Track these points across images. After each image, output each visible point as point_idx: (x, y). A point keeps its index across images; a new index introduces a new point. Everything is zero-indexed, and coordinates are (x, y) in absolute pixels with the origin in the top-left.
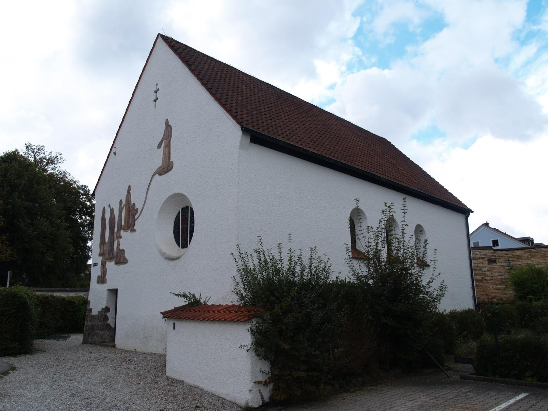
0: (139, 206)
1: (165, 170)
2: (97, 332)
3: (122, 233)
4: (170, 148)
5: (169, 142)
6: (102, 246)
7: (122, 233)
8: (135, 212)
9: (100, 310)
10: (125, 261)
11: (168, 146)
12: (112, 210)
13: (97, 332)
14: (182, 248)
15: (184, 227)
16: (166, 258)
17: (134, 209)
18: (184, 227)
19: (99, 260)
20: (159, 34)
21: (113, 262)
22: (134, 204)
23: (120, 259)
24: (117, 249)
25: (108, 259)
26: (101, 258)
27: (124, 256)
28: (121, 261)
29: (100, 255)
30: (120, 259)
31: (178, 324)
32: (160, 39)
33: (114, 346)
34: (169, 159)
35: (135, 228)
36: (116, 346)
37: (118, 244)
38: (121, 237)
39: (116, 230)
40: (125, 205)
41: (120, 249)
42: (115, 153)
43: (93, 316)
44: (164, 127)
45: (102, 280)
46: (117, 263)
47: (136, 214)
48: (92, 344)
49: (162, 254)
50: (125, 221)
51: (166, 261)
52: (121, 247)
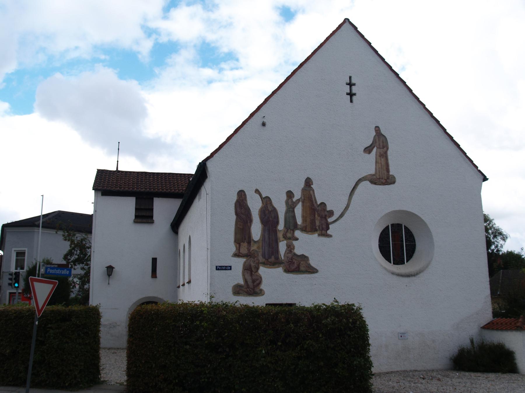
1: (384, 181)
3: (298, 233)
4: (387, 159)
5: (386, 153)
6: (244, 245)
7: (298, 233)
8: (326, 213)
10: (312, 270)
11: (383, 155)
12: (267, 201)
14: (394, 264)
20: (347, 20)
23: (298, 265)
25: (265, 264)
26: (241, 261)
27: (309, 264)
28: (302, 268)
34: (388, 170)
35: (329, 232)
37: (290, 248)
38: (297, 239)
39: (281, 226)
42: (264, 124)
44: (374, 134)
46: (288, 271)
47: (330, 217)
51: (395, 277)
52: (298, 251)
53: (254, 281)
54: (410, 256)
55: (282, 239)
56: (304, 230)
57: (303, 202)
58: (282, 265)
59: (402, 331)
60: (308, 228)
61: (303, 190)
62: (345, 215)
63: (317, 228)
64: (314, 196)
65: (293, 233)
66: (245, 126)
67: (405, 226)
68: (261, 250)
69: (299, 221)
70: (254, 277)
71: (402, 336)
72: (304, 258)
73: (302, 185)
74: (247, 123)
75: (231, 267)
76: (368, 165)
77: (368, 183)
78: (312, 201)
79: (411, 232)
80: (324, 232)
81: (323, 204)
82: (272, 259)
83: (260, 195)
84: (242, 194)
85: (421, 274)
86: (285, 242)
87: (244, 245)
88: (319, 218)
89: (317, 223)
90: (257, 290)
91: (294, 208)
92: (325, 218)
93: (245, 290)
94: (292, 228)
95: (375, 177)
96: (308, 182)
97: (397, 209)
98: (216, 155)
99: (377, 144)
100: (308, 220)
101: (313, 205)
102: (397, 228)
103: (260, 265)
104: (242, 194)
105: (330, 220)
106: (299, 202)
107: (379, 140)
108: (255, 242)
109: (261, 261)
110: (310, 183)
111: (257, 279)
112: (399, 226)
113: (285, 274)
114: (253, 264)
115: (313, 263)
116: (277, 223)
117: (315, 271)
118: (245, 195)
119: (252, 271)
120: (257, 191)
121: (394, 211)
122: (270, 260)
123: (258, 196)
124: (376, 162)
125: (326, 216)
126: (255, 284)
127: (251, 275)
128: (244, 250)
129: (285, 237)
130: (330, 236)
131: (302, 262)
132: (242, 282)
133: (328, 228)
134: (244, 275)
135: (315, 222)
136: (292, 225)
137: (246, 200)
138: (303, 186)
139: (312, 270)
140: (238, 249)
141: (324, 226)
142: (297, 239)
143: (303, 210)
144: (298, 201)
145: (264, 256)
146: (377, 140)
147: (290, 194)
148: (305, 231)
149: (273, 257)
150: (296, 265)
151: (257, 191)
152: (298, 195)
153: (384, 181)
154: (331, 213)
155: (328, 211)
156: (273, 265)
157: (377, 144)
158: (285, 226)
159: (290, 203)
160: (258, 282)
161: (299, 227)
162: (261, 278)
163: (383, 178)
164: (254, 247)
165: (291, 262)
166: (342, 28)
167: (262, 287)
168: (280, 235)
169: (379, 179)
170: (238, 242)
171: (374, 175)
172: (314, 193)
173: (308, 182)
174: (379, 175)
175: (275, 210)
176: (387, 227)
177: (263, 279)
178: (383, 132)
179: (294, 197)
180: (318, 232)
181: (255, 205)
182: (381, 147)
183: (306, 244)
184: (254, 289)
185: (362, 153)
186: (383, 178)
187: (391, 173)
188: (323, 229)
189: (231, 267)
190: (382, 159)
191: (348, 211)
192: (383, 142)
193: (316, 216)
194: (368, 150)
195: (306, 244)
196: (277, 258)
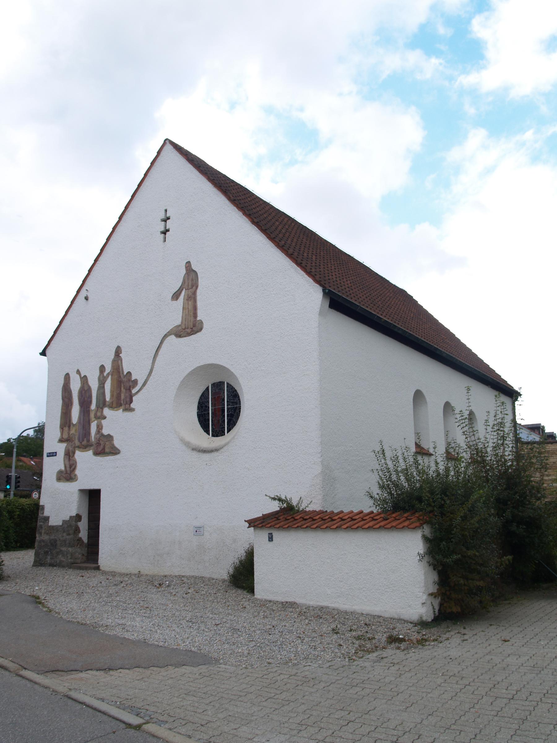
0: (138, 375)
1: (189, 331)
2: (64, 549)
3: (107, 411)
4: (195, 301)
5: (195, 293)
6: (66, 429)
7: (107, 411)
8: (131, 384)
9: (67, 518)
10: (115, 452)
11: (192, 298)
12: (84, 380)
13: (64, 549)
14: (213, 436)
15: (219, 408)
16: (193, 449)
17: (129, 380)
18: (219, 408)
19: (61, 449)
20: (167, 141)
21: (90, 452)
22: (129, 373)
23: (105, 447)
24: (96, 434)
25: (79, 447)
26: (64, 445)
27: (113, 445)
28: (107, 450)
29: (61, 441)
30: (105, 447)
31: (277, 535)
32: (169, 147)
33: (98, 568)
34: (195, 315)
35: (132, 406)
36: (101, 568)
37: (99, 427)
38: (105, 418)
39: (93, 407)
40: (112, 373)
41: (103, 435)
42: (86, 298)
43: (53, 527)
44: (184, 271)
45: (68, 475)
46: (96, 454)
47: (134, 387)
48: (55, 566)
49: (187, 444)
50: (112, 396)
51: (195, 454)
52: (105, 432)
53: (70, 467)
54: (232, 423)
55: (93, 419)
56: (112, 406)
57: (112, 375)
58: (92, 448)
59: (198, 524)
60: (114, 405)
61: (114, 361)
62: (148, 383)
63: (122, 402)
64: (122, 365)
65: (102, 412)
66: (74, 305)
67: (228, 384)
68: (77, 434)
69: (108, 398)
70: (71, 462)
71: (198, 531)
72: (110, 437)
73: (112, 356)
74: (75, 302)
75: (56, 453)
76: (175, 315)
77: (173, 337)
78: (119, 372)
79: (236, 391)
80: (127, 406)
81: (129, 373)
82: (85, 443)
83: (80, 374)
84: (67, 377)
85: (225, 448)
86: (96, 422)
87: (66, 429)
88: (124, 391)
89: (123, 397)
90: (73, 476)
91: (104, 384)
92: (129, 389)
93: (64, 476)
94: (101, 406)
95: (180, 328)
96: (118, 351)
97: (202, 363)
98: (52, 342)
99: (186, 284)
100: (115, 394)
101: (120, 377)
102: (218, 386)
103: (76, 449)
104: (67, 377)
105: (134, 391)
106: (108, 377)
107: (188, 279)
108: (74, 425)
109: (77, 445)
110: (119, 352)
111: (73, 464)
112: (221, 384)
113: (95, 457)
114: (71, 449)
115: (117, 443)
116: (91, 402)
117: (118, 452)
118: (69, 377)
119: (70, 456)
120: (78, 372)
121: (199, 367)
122: (83, 443)
123: (78, 376)
124: (183, 308)
125: (130, 387)
126: (72, 469)
127: (69, 460)
128: (65, 436)
129: (97, 418)
130: (132, 410)
131: (107, 443)
132: (63, 468)
133: (131, 401)
134: (64, 461)
135: (121, 397)
136: (102, 404)
137: (69, 383)
138: (113, 357)
139: (115, 452)
140: (62, 434)
141: (128, 400)
142: (105, 418)
143: (111, 384)
144: (108, 374)
145: (79, 440)
146: (186, 280)
147: (102, 368)
148: (111, 407)
149: (85, 439)
150: (102, 446)
151: (78, 372)
152: (108, 369)
153: (189, 331)
154: (135, 382)
155: (132, 381)
156: (85, 448)
157: (186, 284)
158: (96, 405)
159: (101, 379)
160: (73, 467)
161: (107, 404)
162: (76, 462)
163: (190, 327)
164: (73, 431)
165: (98, 444)
166: (162, 153)
167: (77, 472)
168: (92, 415)
169: (184, 329)
170: (62, 428)
171: (180, 326)
172: (122, 363)
173: (118, 351)
174: (185, 324)
175: (89, 389)
176: (207, 389)
177: (78, 464)
178: (194, 267)
179: (105, 371)
180: (123, 407)
181: (75, 386)
182: (190, 287)
183: (114, 422)
184: (70, 474)
185: (170, 301)
186: (190, 327)
187: (198, 319)
188: (126, 403)
189: (56, 453)
190: (190, 303)
191: (151, 377)
192: (192, 280)
193: (122, 389)
194: (176, 296)
195: (114, 422)
196: (88, 441)
